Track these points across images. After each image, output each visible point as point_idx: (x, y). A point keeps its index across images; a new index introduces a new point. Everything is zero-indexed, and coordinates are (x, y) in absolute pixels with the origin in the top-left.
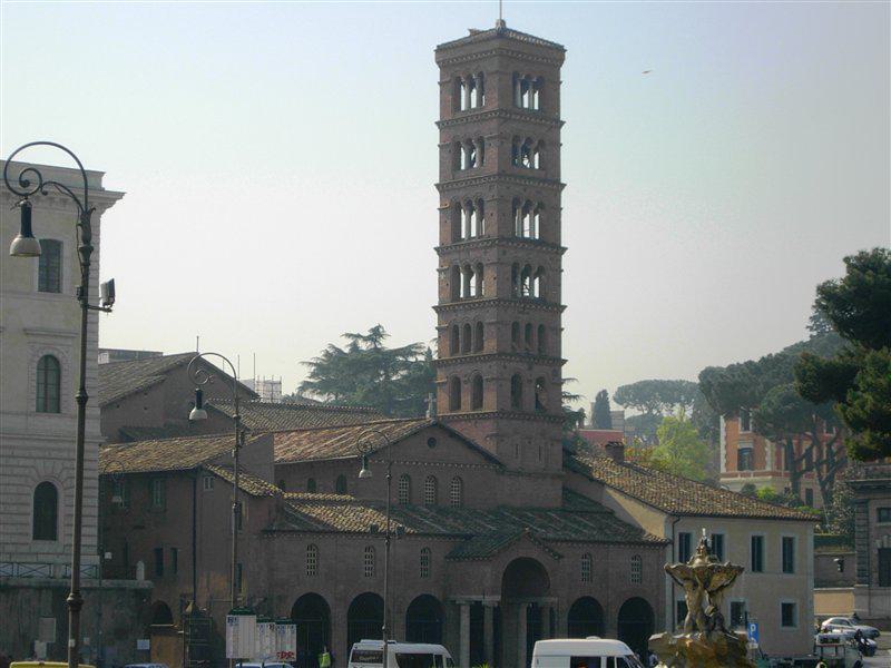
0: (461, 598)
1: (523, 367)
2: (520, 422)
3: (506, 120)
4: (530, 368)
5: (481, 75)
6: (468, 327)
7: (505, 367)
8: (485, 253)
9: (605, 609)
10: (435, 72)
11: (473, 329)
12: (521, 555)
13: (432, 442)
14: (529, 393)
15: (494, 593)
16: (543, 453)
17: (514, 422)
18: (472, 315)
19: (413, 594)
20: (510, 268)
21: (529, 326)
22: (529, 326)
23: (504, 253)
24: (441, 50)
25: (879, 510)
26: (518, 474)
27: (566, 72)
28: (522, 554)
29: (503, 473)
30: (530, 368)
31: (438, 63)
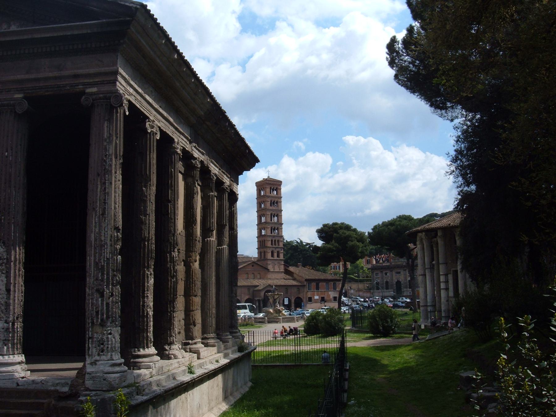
1: (274, 249)
5: (263, 188)
6: (262, 241)
10: (256, 188)
13: (253, 266)
18: (263, 238)
21: (275, 241)
22: (275, 241)
24: (256, 183)
25: (376, 274)
30: (275, 249)
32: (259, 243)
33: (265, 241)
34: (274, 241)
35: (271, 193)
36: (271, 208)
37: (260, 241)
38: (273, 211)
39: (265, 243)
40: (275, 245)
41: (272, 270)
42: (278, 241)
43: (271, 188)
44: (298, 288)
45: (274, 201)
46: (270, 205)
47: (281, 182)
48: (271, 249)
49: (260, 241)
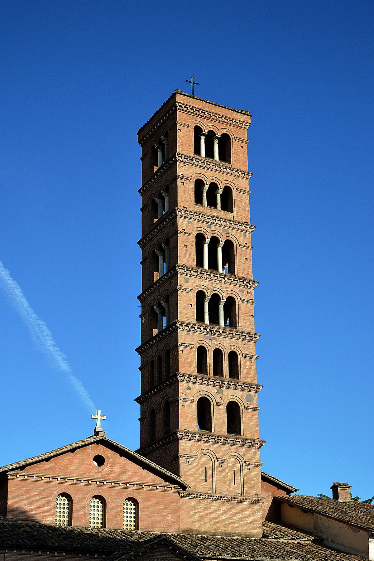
2: (209, 444)
5: (166, 136)
6: (160, 358)
7: (189, 388)
8: (170, 284)
11: (164, 359)
13: (100, 460)
16: (238, 478)
17: (202, 444)
20: (193, 295)
21: (218, 353)
22: (218, 353)
29: (188, 496)
31: (140, 142)
33: (168, 353)
35: (197, 151)
36: (199, 208)
37: (152, 362)
38: (210, 224)
39: (168, 367)
40: (218, 371)
41: (204, 487)
43: (198, 131)
45: (214, 187)
46: (193, 194)
49: (152, 362)
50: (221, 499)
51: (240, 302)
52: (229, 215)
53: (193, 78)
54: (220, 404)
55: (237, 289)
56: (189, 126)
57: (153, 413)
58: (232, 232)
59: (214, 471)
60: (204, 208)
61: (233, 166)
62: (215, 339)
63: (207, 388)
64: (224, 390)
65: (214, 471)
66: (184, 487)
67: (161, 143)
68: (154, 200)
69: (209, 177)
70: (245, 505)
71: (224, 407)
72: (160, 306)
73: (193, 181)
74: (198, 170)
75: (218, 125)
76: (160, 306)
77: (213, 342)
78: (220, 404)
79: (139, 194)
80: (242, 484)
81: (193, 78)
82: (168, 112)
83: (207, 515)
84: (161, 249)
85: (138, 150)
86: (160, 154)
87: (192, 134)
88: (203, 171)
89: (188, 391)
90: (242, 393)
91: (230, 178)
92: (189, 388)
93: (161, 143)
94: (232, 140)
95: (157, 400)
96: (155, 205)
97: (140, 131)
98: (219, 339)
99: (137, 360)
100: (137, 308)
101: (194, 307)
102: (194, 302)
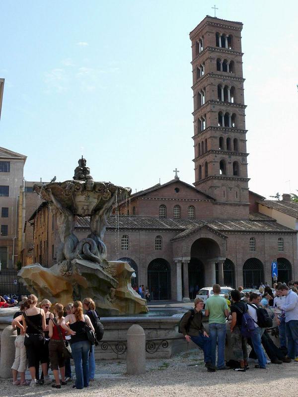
0: (177, 259)
3: (213, 51)
4: (230, 157)
5: (203, 37)
6: (203, 142)
7: (216, 156)
9: (264, 264)
12: (202, 237)
13: (177, 190)
14: (230, 168)
15: (186, 256)
17: (222, 181)
19: (151, 259)
20: (217, 114)
21: (228, 140)
22: (228, 140)
23: (214, 107)
26: (224, 204)
27: (243, 33)
28: (203, 236)
29: (216, 204)
30: (230, 157)
31: (190, 39)
32: (197, 150)
34: (226, 141)
35: (218, 45)
36: (218, 73)
38: (224, 80)
42: (235, 141)
43: (217, 35)
44: (280, 239)
45: (225, 61)
47: (241, 24)
48: (219, 157)
50: (231, 205)
51: (239, 116)
52: (233, 75)
53: (215, 6)
54: (230, 163)
55: (237, 109)
56: (213, 33)
57: (200, 166)
58: (235, 82)
59: (227, 193)
60: (221, 72)
61: (235, 51)
62: (228, 133)
63: (224, 156)
64: (232, 156)
65: (227, 193)
66: (215, 200)
67: (200, 40)
68: (198, 68)
69: (223, 57)
70: (241, 207)
71: (232, 164)
72: (202, 118)
73: (216, 59)
74: (218, 54)
75: (227, 31)
76: (202, 118)
77: (226, 135)
78: (230, 163)
79: (191, 64)
80: (240, 197)
81: (215, 6)
82: (203, 26)
83: (225, 211)
84: (202, 91)
85: (190, 43)
86: (200, 45)
87: (215, 36)
88: (221, 54)
89: (216, 158)
90: (240, 157)
91: (233, 57)
92: (216, 156)
93: (200, 40)
94: (234, 38)
95: (202, 161)
96: (198, 70)
97: (191, 33)
98: (229, 133)
99: (192, 142)
100: (192, 118)
101: (218, 119)
102: (217, 117)
